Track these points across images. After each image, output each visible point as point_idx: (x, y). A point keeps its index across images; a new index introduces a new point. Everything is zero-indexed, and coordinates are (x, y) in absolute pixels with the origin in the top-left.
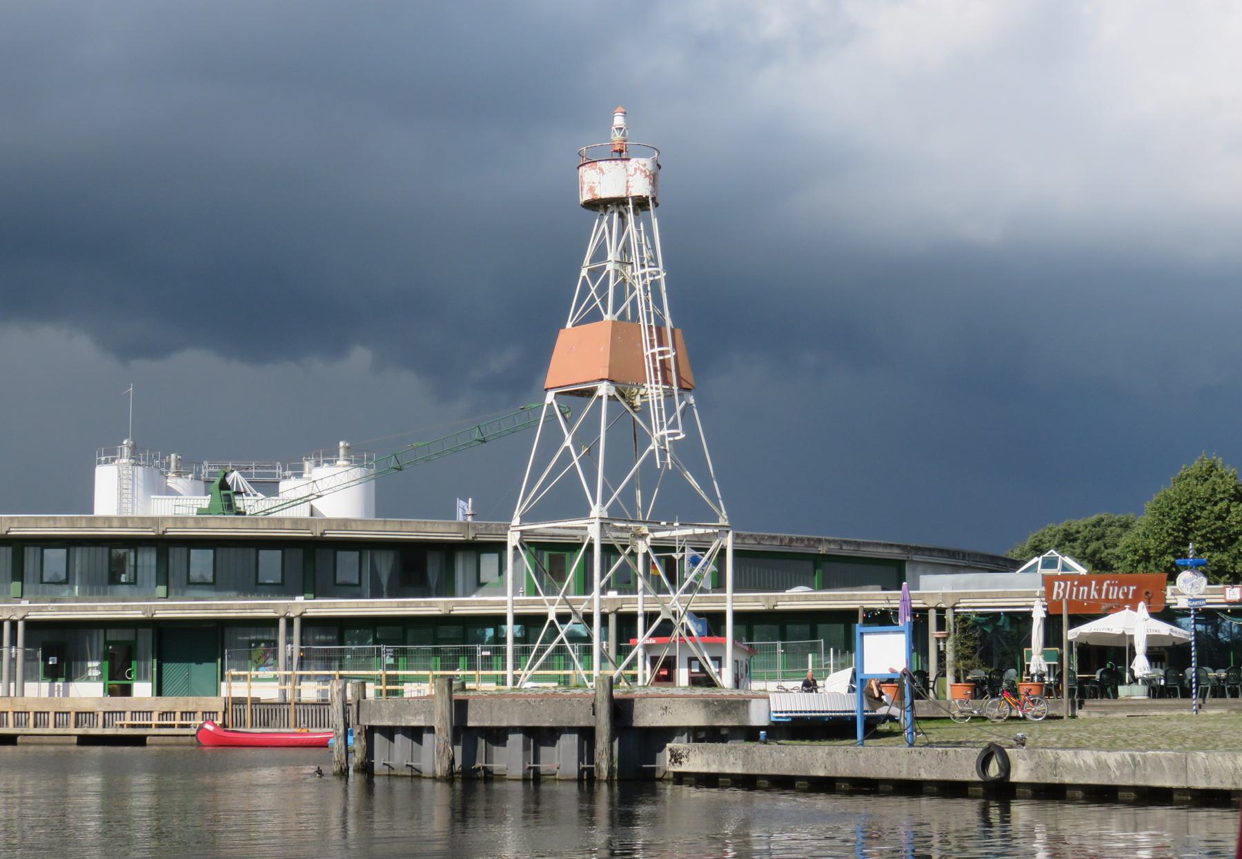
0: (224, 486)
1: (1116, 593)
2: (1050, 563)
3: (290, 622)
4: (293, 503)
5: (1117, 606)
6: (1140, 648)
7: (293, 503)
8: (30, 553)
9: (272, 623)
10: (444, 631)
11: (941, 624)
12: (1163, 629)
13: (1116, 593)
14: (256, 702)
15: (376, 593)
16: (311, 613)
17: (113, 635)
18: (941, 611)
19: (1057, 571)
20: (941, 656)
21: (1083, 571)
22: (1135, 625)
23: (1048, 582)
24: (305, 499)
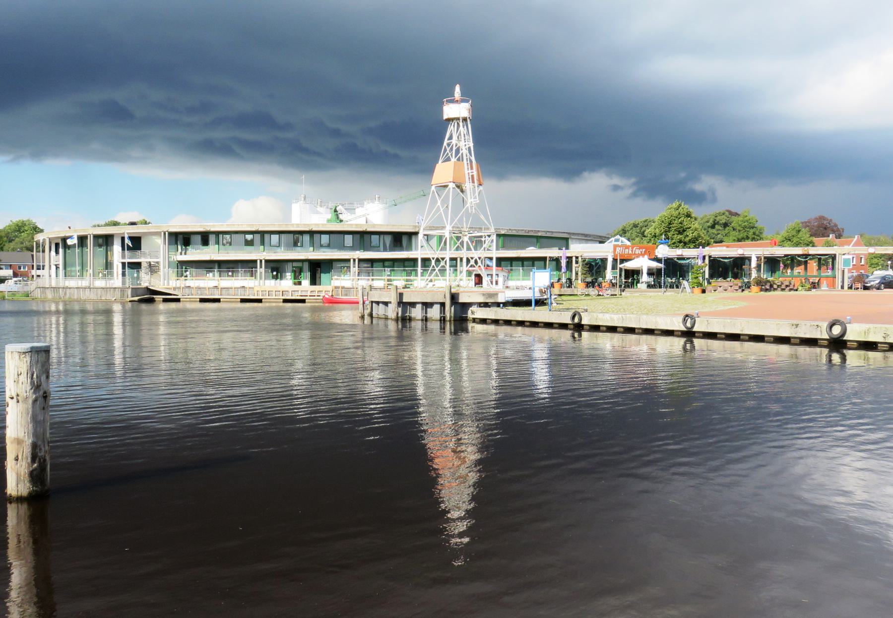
0: (336, 211)
1: (638, 252)
2: (617, 240)
3: (354, 260)
4: (360, 217)
5: (638, 256)
6: (645, 271)
7: (360, 217)
8: (267, 236)
9: (349, 260)
10: (407, 263)
11: (577, 262)
12: (655, 265)
13: (638, 252)
14: (343, 288)
15: (385, 250)
16: (362, 257)
17: (295, 264)
18: (577, 258)
19: (619, 243)
20: (577, 274)
21: (628, 243)
22: (643, 263)
23: (615, 247)
24: (364, 216)
